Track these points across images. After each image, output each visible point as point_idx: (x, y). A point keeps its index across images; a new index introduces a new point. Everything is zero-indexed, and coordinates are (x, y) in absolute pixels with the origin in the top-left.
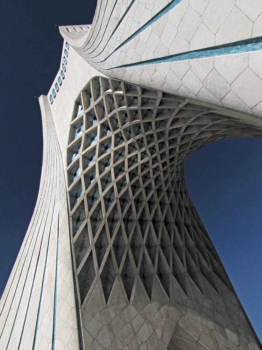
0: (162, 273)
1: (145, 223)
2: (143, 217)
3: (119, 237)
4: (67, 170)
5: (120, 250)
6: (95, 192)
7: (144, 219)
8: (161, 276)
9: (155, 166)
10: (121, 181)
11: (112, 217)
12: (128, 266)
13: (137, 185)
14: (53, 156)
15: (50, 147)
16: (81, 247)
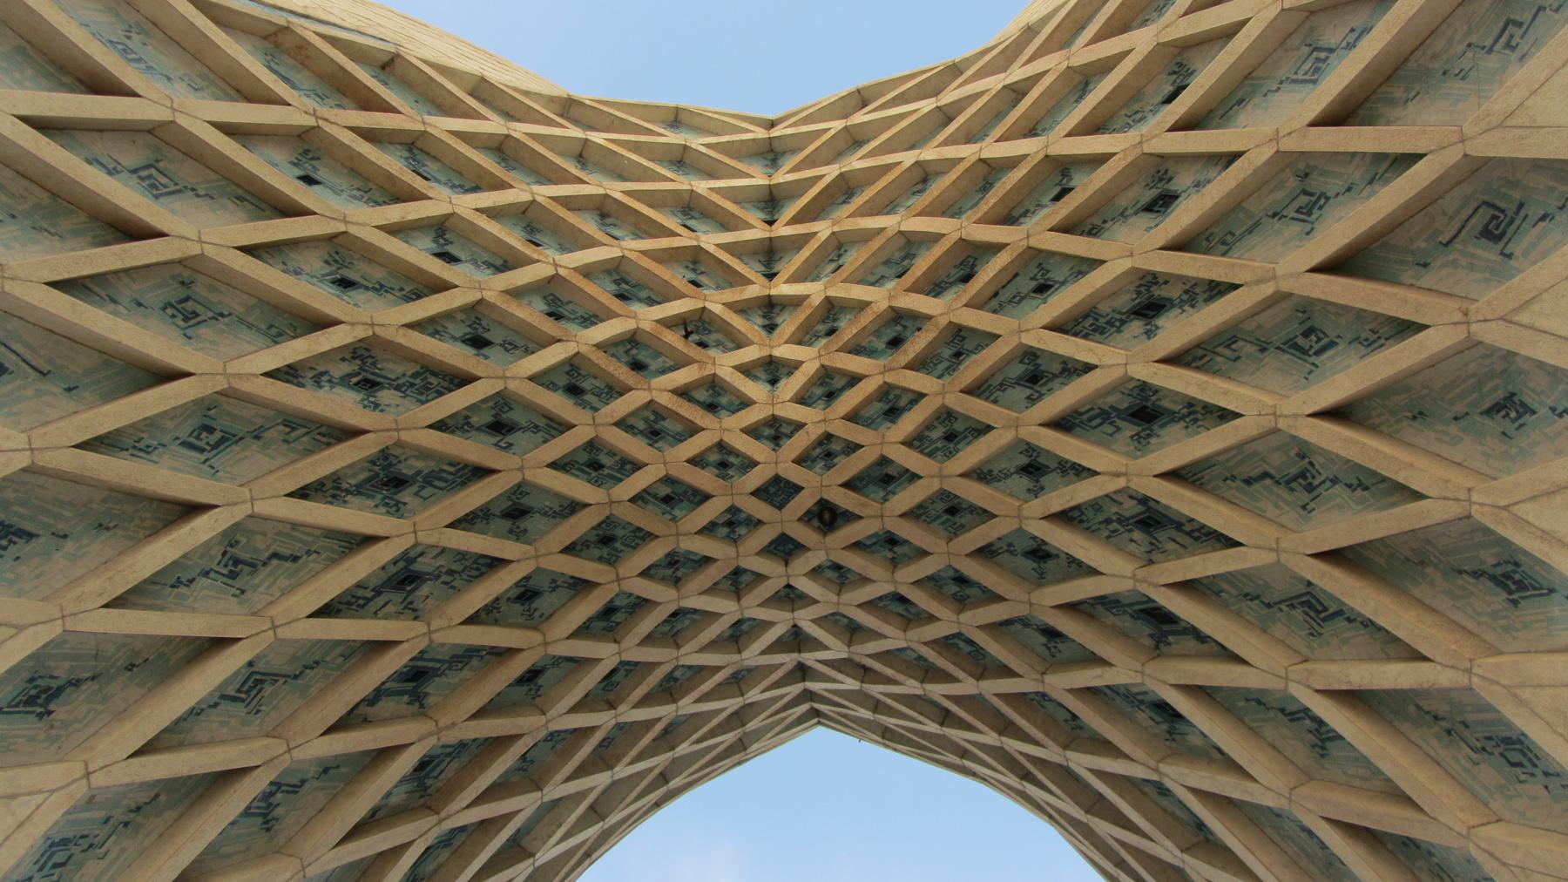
0: (61, 711)
2: (415, 488)
3: (250, 326)
7: (407, 496)
8: (31, 701)
10: (570, 307)
12: (69, 390)
13: (588, 397)
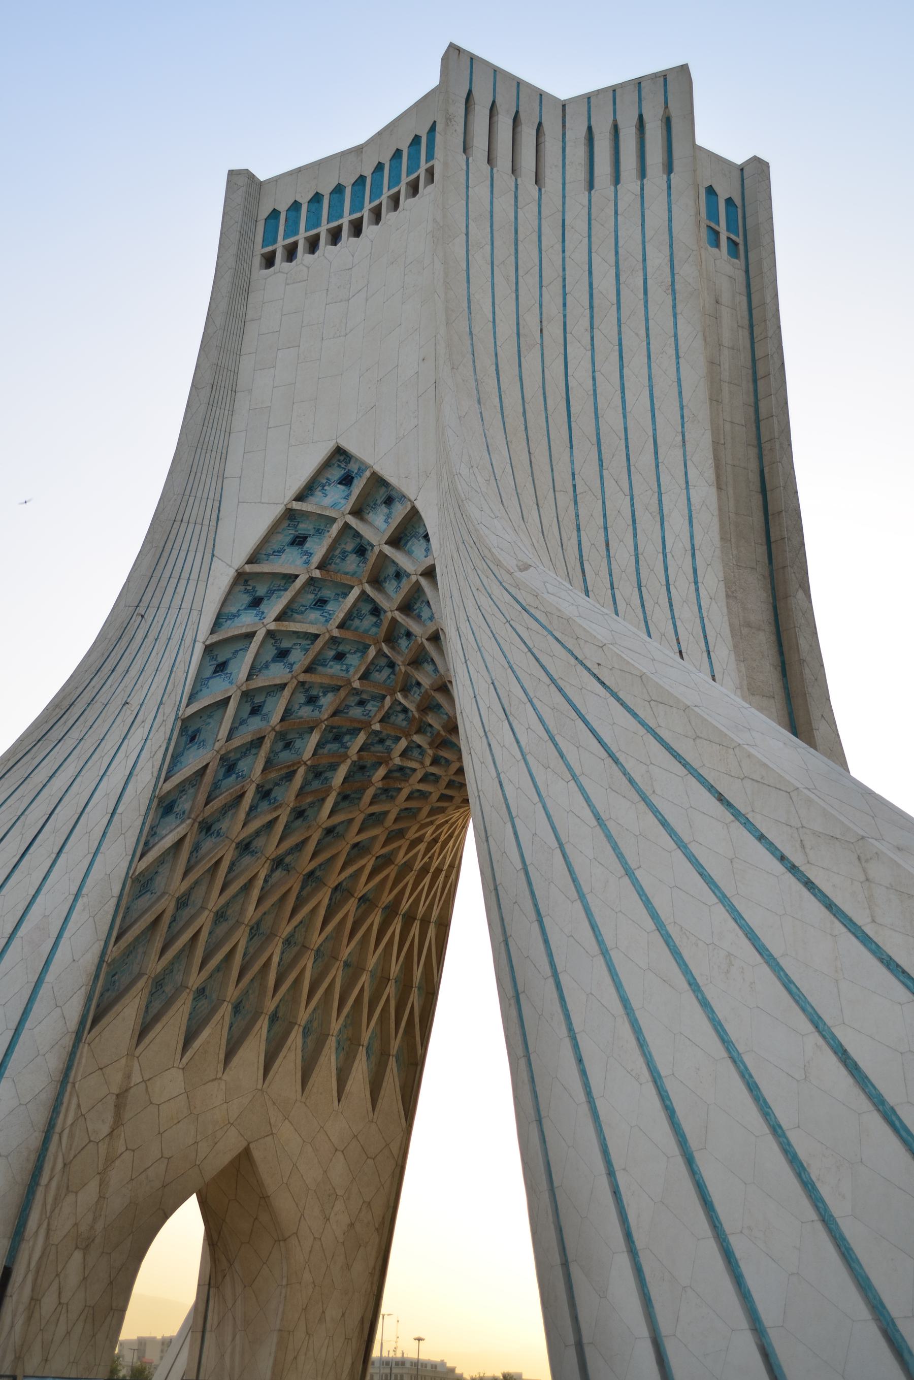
1: (314, 884)
4: (208, 643)
5: (223, 928)
6: (245, 753)
7: (318, 873)
9: (422, 787)
11: (248, 840)
13: (352, 796)
14: (185, 547)
15: (192, 499)
16: (143, 885)
